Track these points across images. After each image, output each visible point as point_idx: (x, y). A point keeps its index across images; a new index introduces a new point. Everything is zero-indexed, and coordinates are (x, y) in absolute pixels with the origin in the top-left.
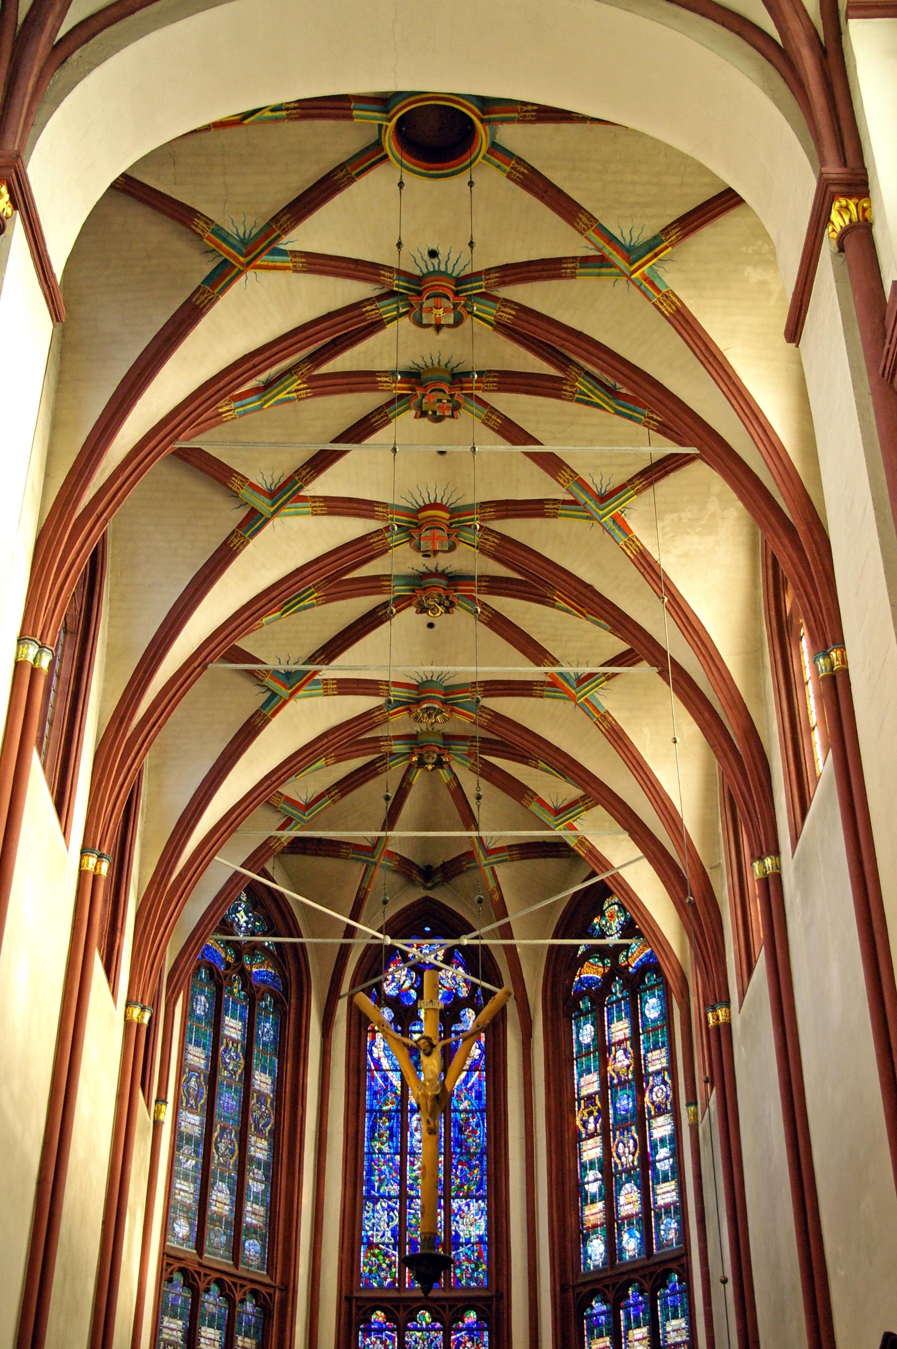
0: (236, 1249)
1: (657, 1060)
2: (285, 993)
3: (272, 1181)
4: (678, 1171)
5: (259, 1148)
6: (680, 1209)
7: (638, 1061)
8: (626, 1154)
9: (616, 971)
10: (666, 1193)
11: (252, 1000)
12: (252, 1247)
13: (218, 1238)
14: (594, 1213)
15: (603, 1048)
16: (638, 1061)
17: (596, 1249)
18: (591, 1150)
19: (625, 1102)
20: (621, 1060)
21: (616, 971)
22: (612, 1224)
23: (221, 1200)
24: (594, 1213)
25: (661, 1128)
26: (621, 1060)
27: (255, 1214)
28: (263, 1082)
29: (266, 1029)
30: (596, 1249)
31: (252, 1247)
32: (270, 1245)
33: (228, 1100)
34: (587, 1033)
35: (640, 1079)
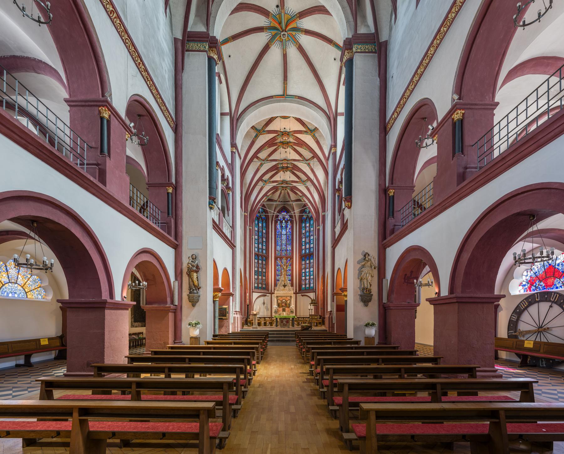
0: (262, 251)
1: (312, 229)
2: (266, 220)
3: (266, 244)
4: (313, 243)
5: (264, 240)
6: (313, 247)
7: (310, 229)
8: (307, 241)
9: (308, 217)
10: (312, 246)
11: (262, 221)
12: (264, 251)
13: (260, 251)
14: (303, 247)
15: (306, 227)
16: (310, 229)
17: (304, 251)
18: (304, 240)
19: (308, 234)
20: (308, 229)
21: (308, 217)
22: (306, 249)
23: (260, 246)
24: (303, 247)
25: (312, 238)
26: (308, 229)
27: (264, 247)
28: (264, 231)
29: (264, 224)
30: (304, 251)
31: (264, 251)
32: (266, 251)
33: (260, 234)
34: (304, 225)
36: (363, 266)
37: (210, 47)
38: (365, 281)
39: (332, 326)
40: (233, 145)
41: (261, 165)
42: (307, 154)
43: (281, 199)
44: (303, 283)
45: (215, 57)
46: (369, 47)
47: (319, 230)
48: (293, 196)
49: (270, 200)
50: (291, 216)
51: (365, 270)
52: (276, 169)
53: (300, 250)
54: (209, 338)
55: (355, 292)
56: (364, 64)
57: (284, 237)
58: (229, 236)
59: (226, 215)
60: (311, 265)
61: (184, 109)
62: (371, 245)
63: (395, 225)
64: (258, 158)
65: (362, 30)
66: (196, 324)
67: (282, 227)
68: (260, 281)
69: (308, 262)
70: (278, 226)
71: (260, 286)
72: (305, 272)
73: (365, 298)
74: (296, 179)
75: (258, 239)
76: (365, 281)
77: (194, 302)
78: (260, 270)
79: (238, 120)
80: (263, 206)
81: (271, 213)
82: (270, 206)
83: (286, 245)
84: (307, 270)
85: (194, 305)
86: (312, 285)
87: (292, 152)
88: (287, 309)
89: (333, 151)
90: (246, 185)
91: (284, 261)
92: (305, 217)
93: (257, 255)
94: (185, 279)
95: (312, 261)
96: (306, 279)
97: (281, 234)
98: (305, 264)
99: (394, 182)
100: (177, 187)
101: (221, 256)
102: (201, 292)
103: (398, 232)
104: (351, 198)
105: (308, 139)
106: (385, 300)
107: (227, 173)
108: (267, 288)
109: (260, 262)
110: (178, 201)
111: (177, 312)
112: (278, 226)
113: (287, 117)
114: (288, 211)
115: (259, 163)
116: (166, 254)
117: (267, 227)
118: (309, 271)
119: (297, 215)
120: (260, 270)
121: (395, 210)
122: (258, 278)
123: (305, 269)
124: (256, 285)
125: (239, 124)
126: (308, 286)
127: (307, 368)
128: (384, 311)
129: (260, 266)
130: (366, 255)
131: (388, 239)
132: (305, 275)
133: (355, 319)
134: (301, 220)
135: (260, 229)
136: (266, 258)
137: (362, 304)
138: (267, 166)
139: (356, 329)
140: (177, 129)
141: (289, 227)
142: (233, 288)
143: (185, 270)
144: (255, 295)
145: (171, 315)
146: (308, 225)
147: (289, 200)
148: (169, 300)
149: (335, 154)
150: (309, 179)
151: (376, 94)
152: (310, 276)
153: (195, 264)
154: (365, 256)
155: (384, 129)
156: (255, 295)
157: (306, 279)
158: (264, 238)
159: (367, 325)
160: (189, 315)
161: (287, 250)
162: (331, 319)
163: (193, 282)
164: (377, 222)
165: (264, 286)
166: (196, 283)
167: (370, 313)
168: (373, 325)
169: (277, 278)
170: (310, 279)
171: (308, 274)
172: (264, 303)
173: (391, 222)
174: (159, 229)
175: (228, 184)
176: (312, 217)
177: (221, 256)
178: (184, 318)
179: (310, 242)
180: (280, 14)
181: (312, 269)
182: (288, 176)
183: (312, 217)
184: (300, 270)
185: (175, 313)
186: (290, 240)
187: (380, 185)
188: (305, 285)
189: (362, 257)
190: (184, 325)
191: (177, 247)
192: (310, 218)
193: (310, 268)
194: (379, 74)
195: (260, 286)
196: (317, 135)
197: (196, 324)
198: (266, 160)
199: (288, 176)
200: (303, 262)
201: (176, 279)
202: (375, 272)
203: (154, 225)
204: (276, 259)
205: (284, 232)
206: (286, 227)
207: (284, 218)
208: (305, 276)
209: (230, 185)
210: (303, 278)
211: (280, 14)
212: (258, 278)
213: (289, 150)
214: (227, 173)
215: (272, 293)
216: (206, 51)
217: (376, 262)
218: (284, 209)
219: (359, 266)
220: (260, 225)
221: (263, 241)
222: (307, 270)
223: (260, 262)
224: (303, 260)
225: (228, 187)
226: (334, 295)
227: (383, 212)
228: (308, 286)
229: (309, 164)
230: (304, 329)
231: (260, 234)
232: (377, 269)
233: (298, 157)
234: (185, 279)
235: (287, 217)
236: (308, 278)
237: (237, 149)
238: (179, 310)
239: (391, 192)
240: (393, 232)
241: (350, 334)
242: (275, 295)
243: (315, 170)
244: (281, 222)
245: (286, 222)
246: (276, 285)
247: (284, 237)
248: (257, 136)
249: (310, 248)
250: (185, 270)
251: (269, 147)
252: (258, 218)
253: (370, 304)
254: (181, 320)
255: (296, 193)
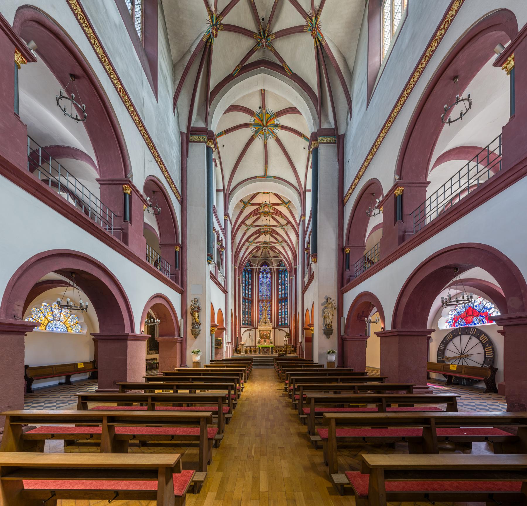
1: (286, 279)
2: (251, 272)
5: (250, 287)
8: (283, 288)
9: (283, 269)
10: (286, 292)
12: (250, 296)
14: (280, 293)
15: (282, 277)
17: (280, 296)
18: (280, 287)
19: (283, 283)
20: (283, 279)
21: (283, 269)
23: (247, 292)
24: (280, 293)
25: (286, 285)
26: (283, 279)
27: (250, 293)
28: (250, 281)
29: (250, 275)
30: (280, 296)
31: (250, 296)
33: (247, 283)
34: (280, 276)
35: (285, 280)
36: (326, 307)
37: (208, 139)
38: (327, 319)
39: (302, 353)
40: (226, 214)
41: (248, 229)
42: (283, 221)
43: (262, 256)
44: (280, 320)
45: (212, 146)
46: (331, 139)
47: (292, 279)
48: (272, 254)
49: (254, 257)
50: (270, 269)
51: (327, 310)
52: (258, 233)
53: (278, 295)
54: (208, 363)
55: (320, 327)
56: (327, 152)
57: (265, 285)
58: (223, 284)
59: (221, 268)
60: (286, 306)
61: (188, 186)
62: (332, 292)
63: (350, 276)
64: (245, 224)
65: (325, 126)
66: (198, 352)
67: (263, 277)
68: (247, 319)
69: (283, 304)
70: (261, 277)
71: (247, 322)
72: (281, 312)
73: (327, 332)
74: (275, 241)
75: (245, 287)
76: (327, 319)
77: (196, 335)
78: (247, 310)
79: (229, 195)
80: (249, 261)
81: (255, 266)
82: (254, 261)
83: (266, 291)
84: (283, 310)
85: (196, 338)
86: (286, 322)
87: (271, 219)
88: (267, 340)
89: (302, 219)
90: (236, 245)
91: (265, 303)
92: (281, 269)
93: (244, 299)
94: (189, 317)
95: (286, 303)
96: (282, 317)
97: (263, 283)
98: (281, 306)
99: (350, 242)
100: (183, 247)
101: (216, 300)
102: (201, 327)
103: (353, 281)
104: (316, 255)
105: (283, 209)
106: (342, 334)
107: (221, 236)
108: (252, 324)
109: (247, 304)
110: (184, 258)
111: (183, 342)
112: (261, 277)
113: (267, 192)
114: (268, 265)
115: (246, 228)
116: (174, 298)
117: (252, 277)
118: (285, 311)
119: (275, 268)
120: (247, 310)
121: (350, 264)
122: (245, 317)
123: (281, 309)
124: (244, 322)
125: (230, 198)
126: (283, 322)
127: (283, 386)
128: (342, 342)
129: (247, 307)
130: (328, 299)
131: (345, 286)
132: (282, 314)
133: (320, 348)
134: (278, 272)
135: (247, 279)
136: (251, 301)
137: (325, 336)
138: (252, 230)
139: (320, 356)
140: (182, 202)
141: (269, 277)
142: (226, 324)
143: (189, 311)
144: (243, 330)
145: (178, 345)
146: (283, 276)
147: (269, 256)
148: (176, 333)
149: (304, 221)
150: (284, 240)
151: (336, 175)
152: (285, 315)
153: (196, 306)
154: (327, 299)
155: (342, 202)
156: (243, 330)
157: (282, 317)
158: (250, 286)
159: (329, 353)
160: (192, 345)
161: (267, 295)
162: (301, 348)
163: (195, 319)
164: (336, 273)
165: (250, 323)
166: (197, 320)
167: (332, 343)
168: (333, 352)
169: (260, 316)
170: (285, 317)
171: (283, 313)
172: (250, 336)
173: (347, 273)
174: (169, 279)
175: (222, 244)
176: (286, 269)
177: (216, 300)
178: (188, 347)
179: (285, 289)
180: (262, 113)
181: (286, 310)
182: (268, 238)
183: (286, 269)
184: (278, 310)
185: (181, 343)
186: (270, 287)
187: (339, 245)
188: (282, 322)
189: (325, 300)
190: (188, 353)
191: (183, 293)
192: (285, 271)
193: (285, 309)
194: (338, 160)
195: (247, 322)
196: (290, 206)
197: (198, 352)
198: (251, 225)
199: (268, 238)
200: (280, 304)
201: (182, 317)
202: (335, 312)
203: (165, 276)
204: (259, 302)
205: (265, 281)
206: (267, 277)
207: (265, 271)
208: (282, 315)
209: (224, 245)
210: (280, 317)
211: (262, 113)
212: (245, 317)
213: (269, 218)
214: (221, 236)
215: (255, 328)
216: (205, 142)
217: (335, 304)
218: (265, 263)
219: (323, 307)
220: (247, 276)
221: (249, 288)
222: (283, 310)
223: (247, 304)
224: (279, 303)
225: (222, 247)
226: (303, 329)
227: (341, 266)
228: (283, 322)
229: (284, 229)
230: (281, 355)
231: (247, 283)
232: (336, 309)
233: (275, 223)
234: (189, 317)
235: (268, 269)
236: (283, 316)
237: (229, 217)
238: (184, 342)
239: (348, 251)
240: (349, 281)
241: (316, 360)
242: (258, 329)
243: (289, 233)
244: (263, 274)
245: (267, 273)
246: (259, 322)
247: (265, 285)
248: (244, 208)
249: (285, 293)
250: (189, 311)
251: (254, 216)
252: (245, 271)
253: (331, 336)
254: (186, 349)
255: (274, 251)
